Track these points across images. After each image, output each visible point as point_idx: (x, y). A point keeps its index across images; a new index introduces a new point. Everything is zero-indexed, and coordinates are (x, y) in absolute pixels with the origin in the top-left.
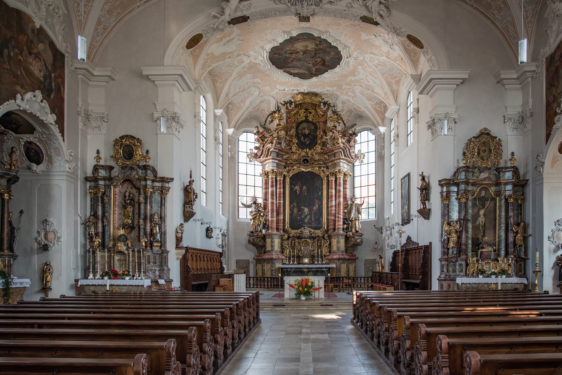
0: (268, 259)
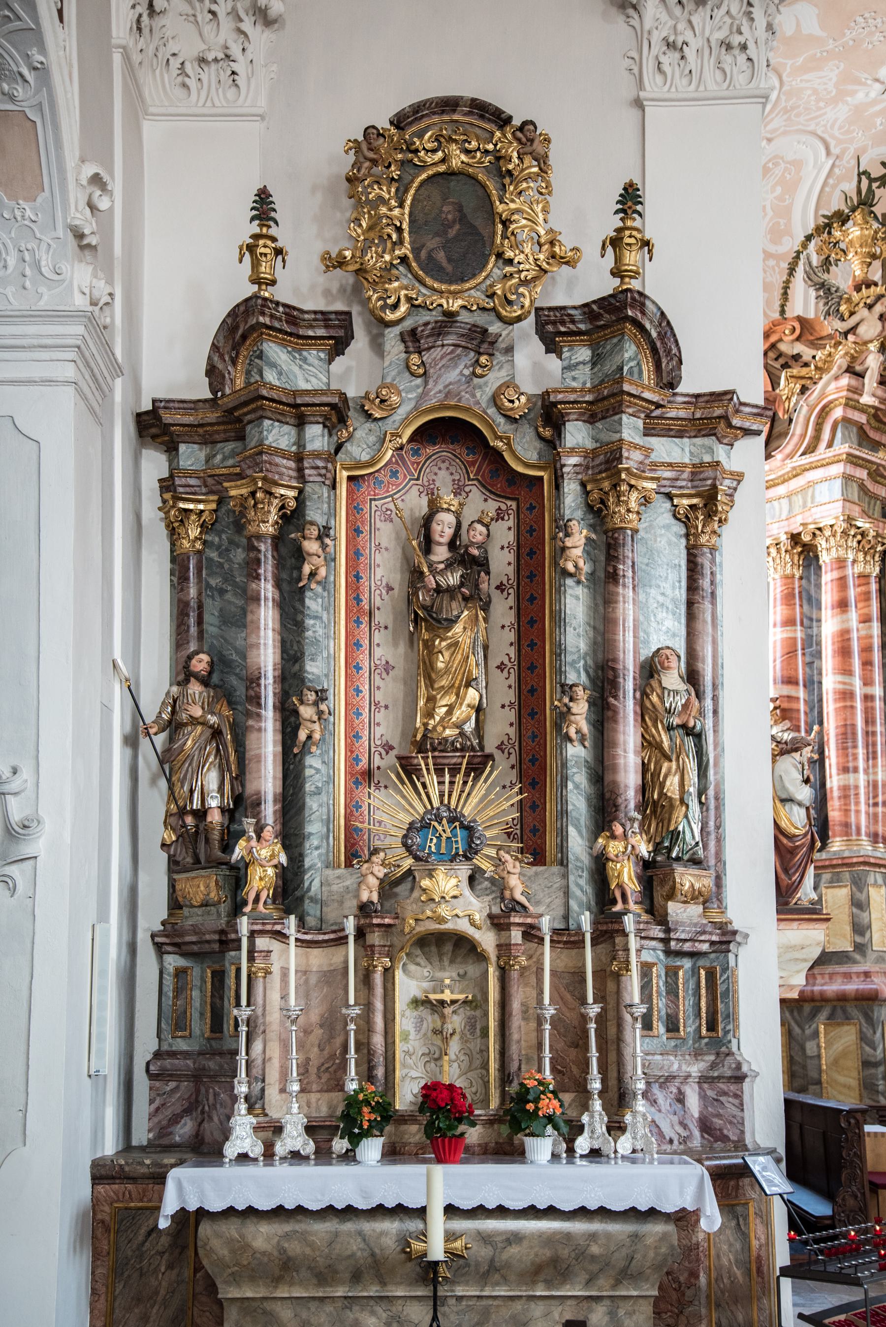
0: (842, 998)
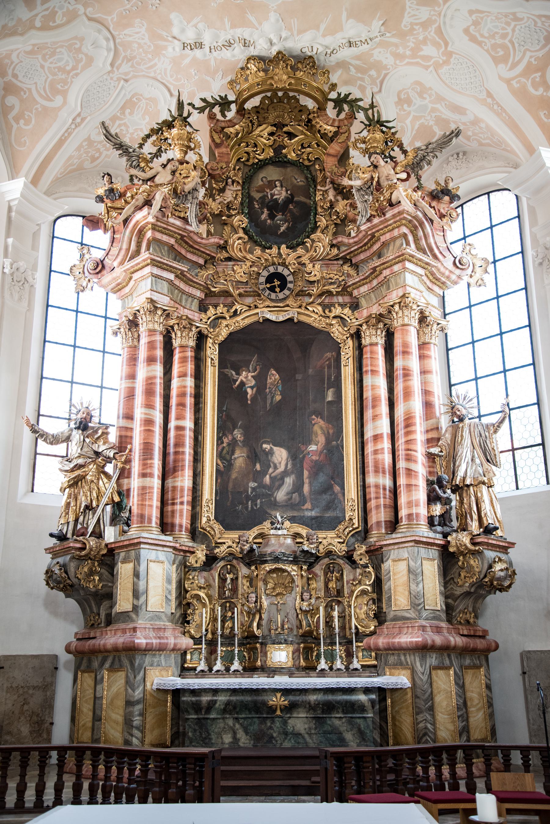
0: (116, 649)
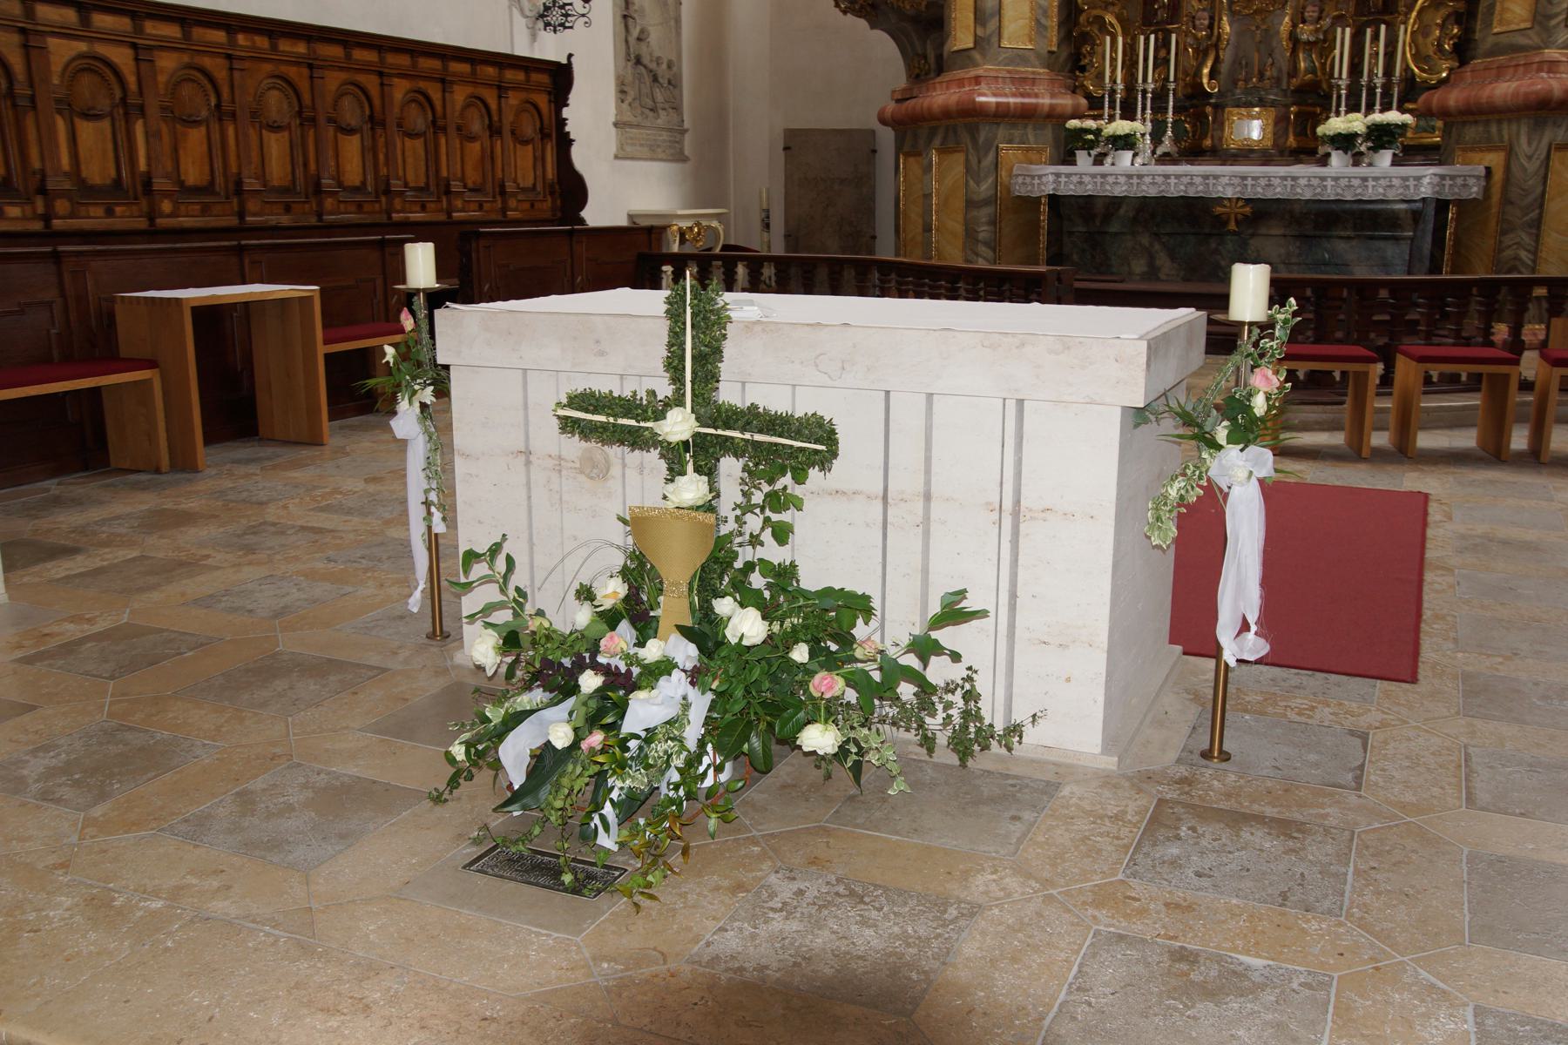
0: (946, 114)
